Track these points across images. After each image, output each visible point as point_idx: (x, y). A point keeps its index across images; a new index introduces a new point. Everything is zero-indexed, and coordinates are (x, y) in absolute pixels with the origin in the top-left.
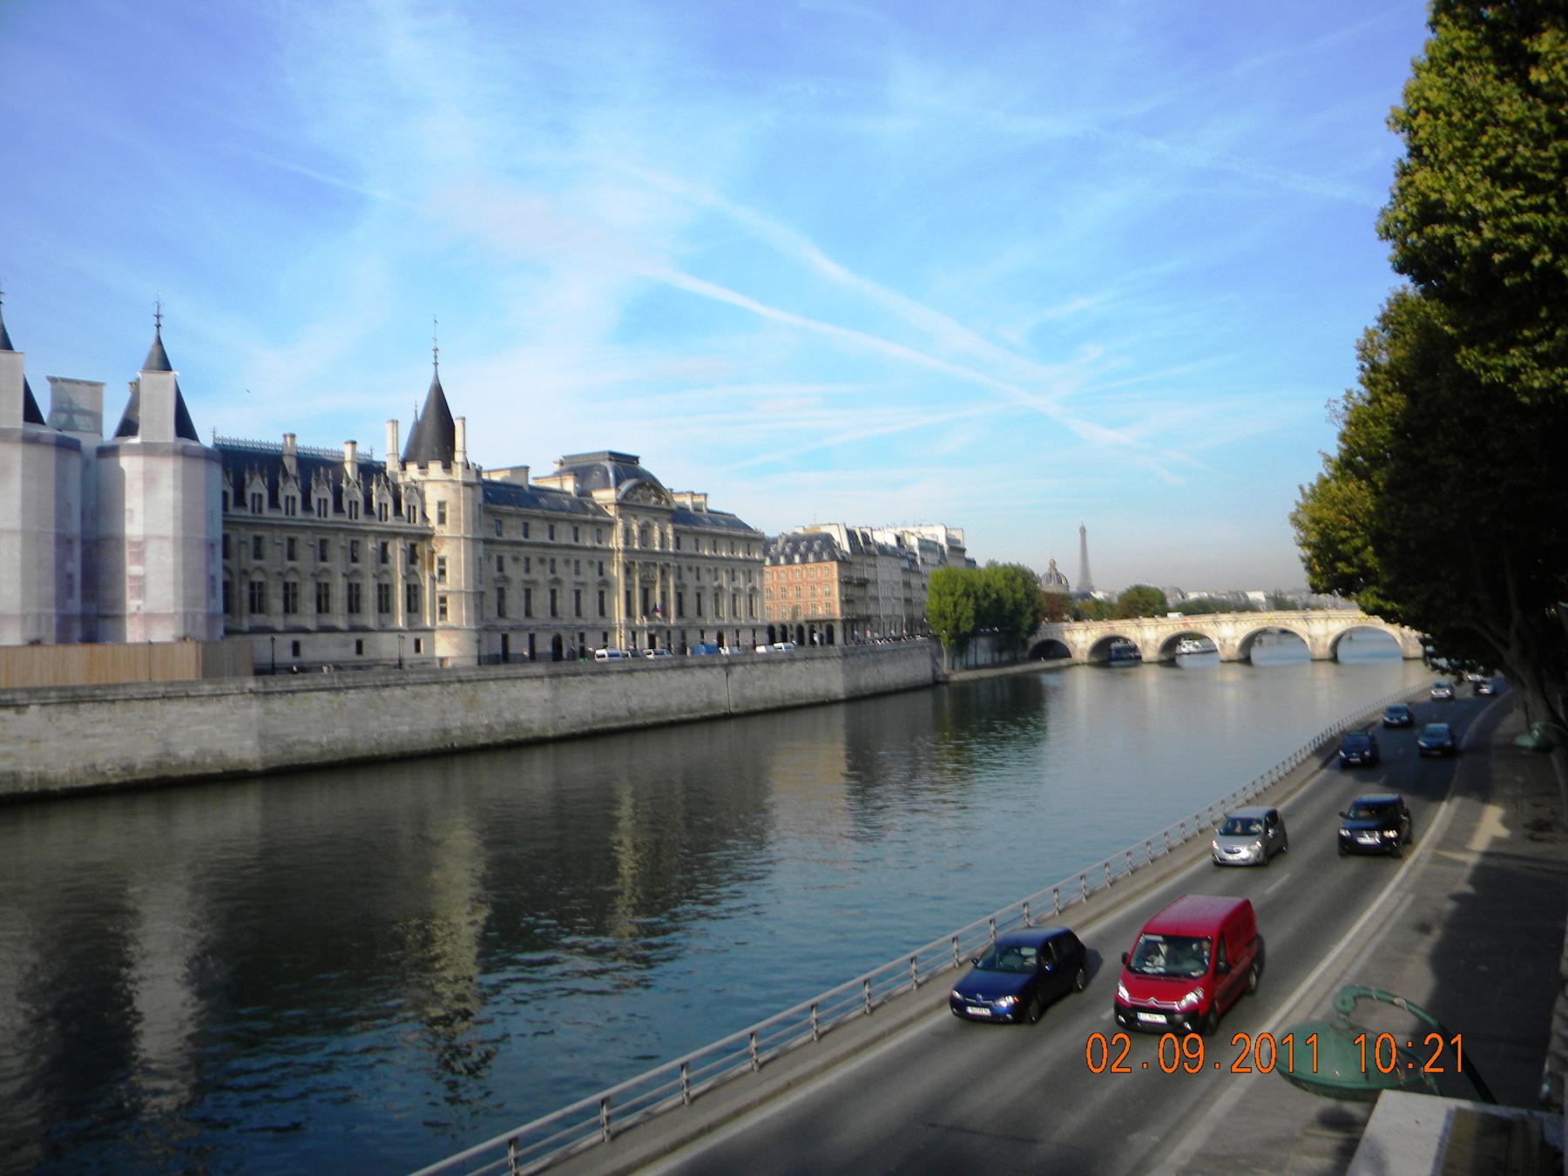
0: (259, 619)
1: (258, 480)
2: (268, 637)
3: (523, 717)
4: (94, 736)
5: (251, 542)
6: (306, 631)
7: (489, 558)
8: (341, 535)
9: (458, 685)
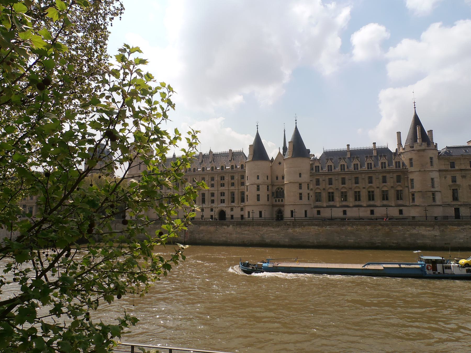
0: (331, 203)
1: (329, 161)
2: (330, 209)
3: (419, 241)
4: (244, 234)
5: (327, 180)
6: (348, 207)
7: (445, 178)
8: (363, 175)
9: (380, 227)
